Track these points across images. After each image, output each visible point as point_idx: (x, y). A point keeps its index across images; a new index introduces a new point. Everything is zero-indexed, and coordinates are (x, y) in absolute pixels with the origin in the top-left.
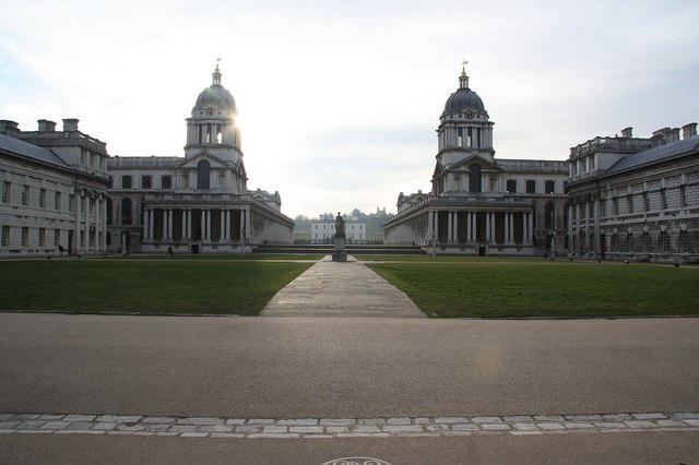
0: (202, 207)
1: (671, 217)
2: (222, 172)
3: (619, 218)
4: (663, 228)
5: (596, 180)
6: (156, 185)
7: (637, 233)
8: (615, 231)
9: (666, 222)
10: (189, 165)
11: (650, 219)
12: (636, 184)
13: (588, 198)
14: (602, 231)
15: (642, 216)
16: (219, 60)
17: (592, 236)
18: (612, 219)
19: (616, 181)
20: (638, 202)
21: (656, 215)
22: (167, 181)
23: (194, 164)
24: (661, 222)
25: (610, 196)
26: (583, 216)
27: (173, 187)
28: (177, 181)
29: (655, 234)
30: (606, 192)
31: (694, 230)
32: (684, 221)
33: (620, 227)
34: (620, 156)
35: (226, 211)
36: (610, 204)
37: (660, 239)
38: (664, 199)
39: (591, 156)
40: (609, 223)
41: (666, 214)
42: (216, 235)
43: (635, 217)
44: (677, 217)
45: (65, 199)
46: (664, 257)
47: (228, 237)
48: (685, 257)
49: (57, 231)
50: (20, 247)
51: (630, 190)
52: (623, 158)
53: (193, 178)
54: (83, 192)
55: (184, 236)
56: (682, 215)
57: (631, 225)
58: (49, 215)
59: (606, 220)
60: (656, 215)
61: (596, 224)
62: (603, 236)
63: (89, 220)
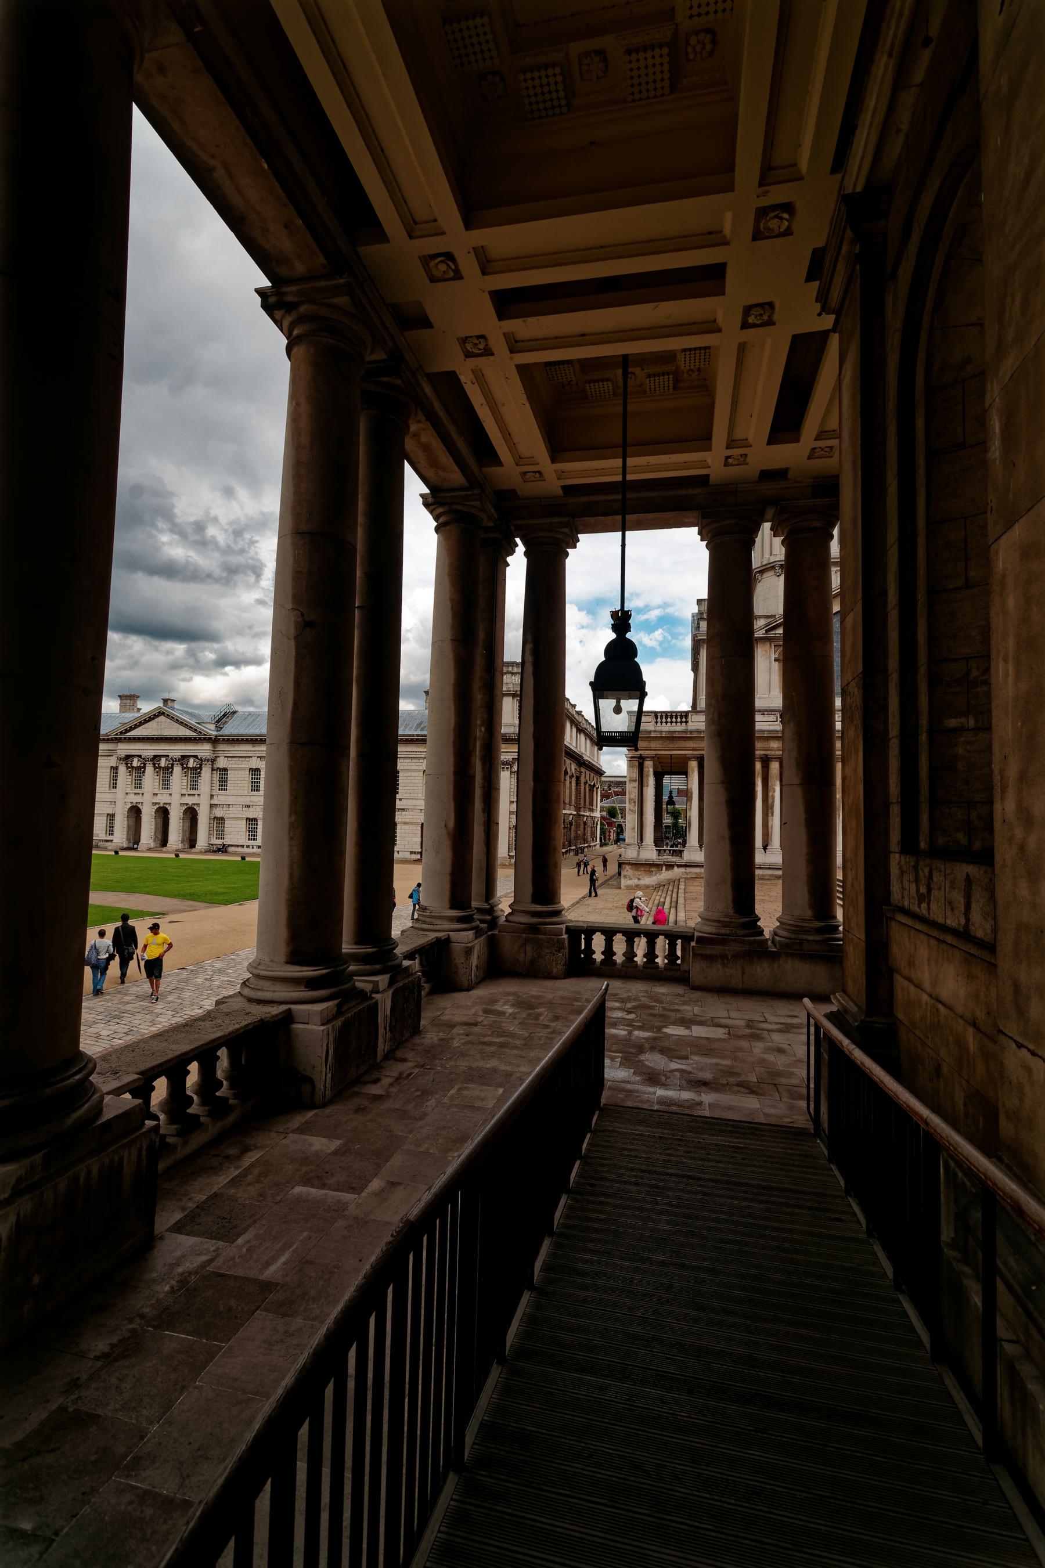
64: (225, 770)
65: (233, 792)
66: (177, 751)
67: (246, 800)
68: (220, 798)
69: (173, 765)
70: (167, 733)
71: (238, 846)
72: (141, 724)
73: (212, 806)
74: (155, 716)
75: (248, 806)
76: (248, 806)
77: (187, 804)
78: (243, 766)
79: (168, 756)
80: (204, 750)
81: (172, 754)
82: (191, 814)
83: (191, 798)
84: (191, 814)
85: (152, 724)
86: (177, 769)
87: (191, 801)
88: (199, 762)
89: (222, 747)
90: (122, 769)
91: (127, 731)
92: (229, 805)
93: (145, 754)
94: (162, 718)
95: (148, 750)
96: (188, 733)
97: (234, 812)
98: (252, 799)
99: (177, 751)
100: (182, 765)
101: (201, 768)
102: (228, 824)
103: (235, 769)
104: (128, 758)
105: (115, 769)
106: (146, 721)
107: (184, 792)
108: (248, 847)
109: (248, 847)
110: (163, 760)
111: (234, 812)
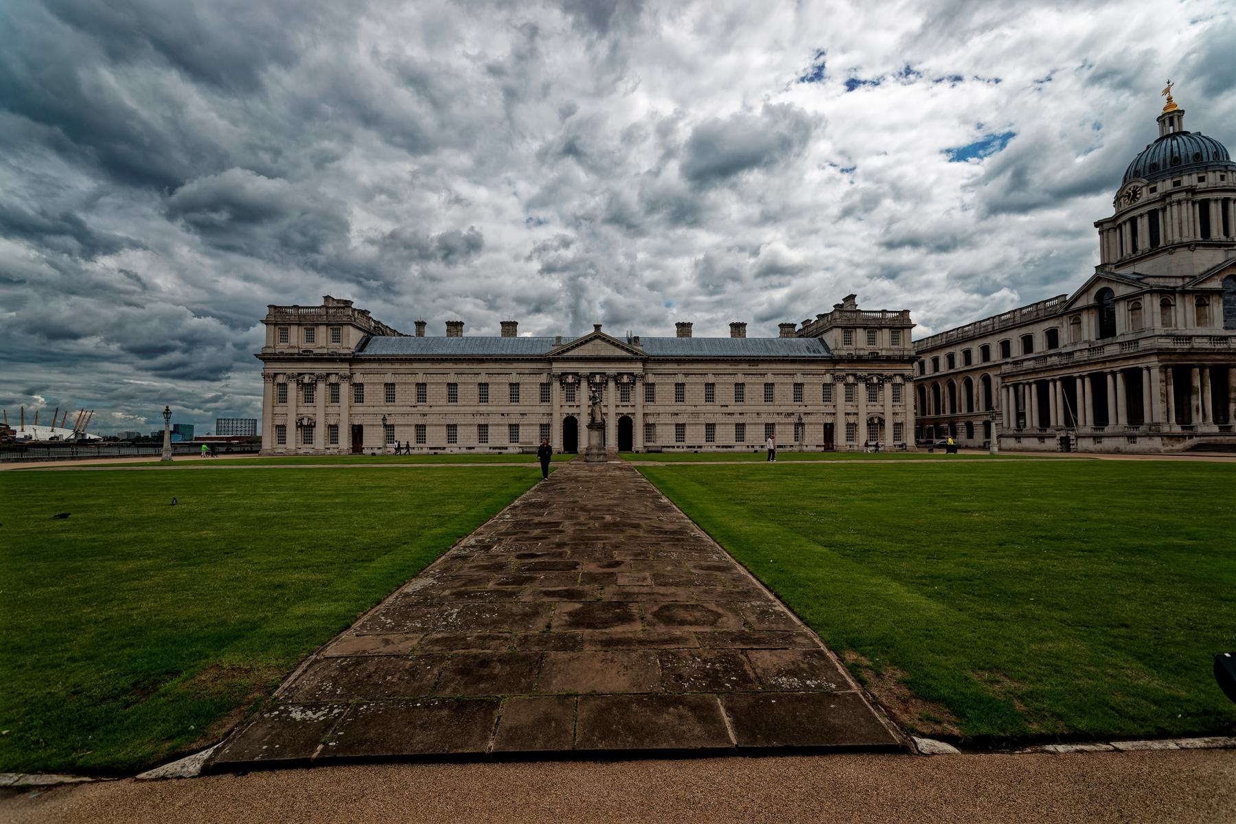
0: (1074, 372)
2: (1134, 303)
6: (1040, 345)
10: (1080, 304)
16: (1167, 91)
22: (1052, 336)
23: (1089, 299)
27: (1061, 344)
28: (1065, 334)
35: (1114, 374)
42: (1101, 417)
45: (813, 392)
47: (1123, 420)
49: (799, 425)
50: (733, 442)
53: (1089, 324)
54: (851, 380)
55: (1053, 423)
58: (783, 409)
63: (864, 407)
64: (653, 384)
65: (660, 403)
66: (612, 369)
67: (675, 409)
68: (651, 408)
69: (607, 381)
70: (603, 353)
71: (669, 447)
72: (577, 346)
73: (644, 414)
74: (591, 339)
75: (677, 414)
76: (677, 414)
77: (621, 414)
78: (669, 381)
79: (604, 374)
80: (637, 368)
81: (608, 372)
82: (625, 425)
83: (624, 408)
84: (625, 425)
85: (589, 346)
86: (612, 385)
87: (625, 411)
88: (632, 378)
89: (649, 366)
90: (556, 385)
91: (563, 352)
92: (659, 414)
93: (581, 372)
94: (598, 341)
95: (585, 369)
96: (624, 354)
97: (663, 419)
98: (679, 408)
99: (612, 369)
100: (616, 381)
101: (634, 383)
102: (659, 429)
103: (662, 384)
104: (564, 374)
105: (545, 387)
106: (582, 344)
107: (618, 403)
108: (678, 447)
109: (678, 447)
110: (598, 377)
111: (663, 419)
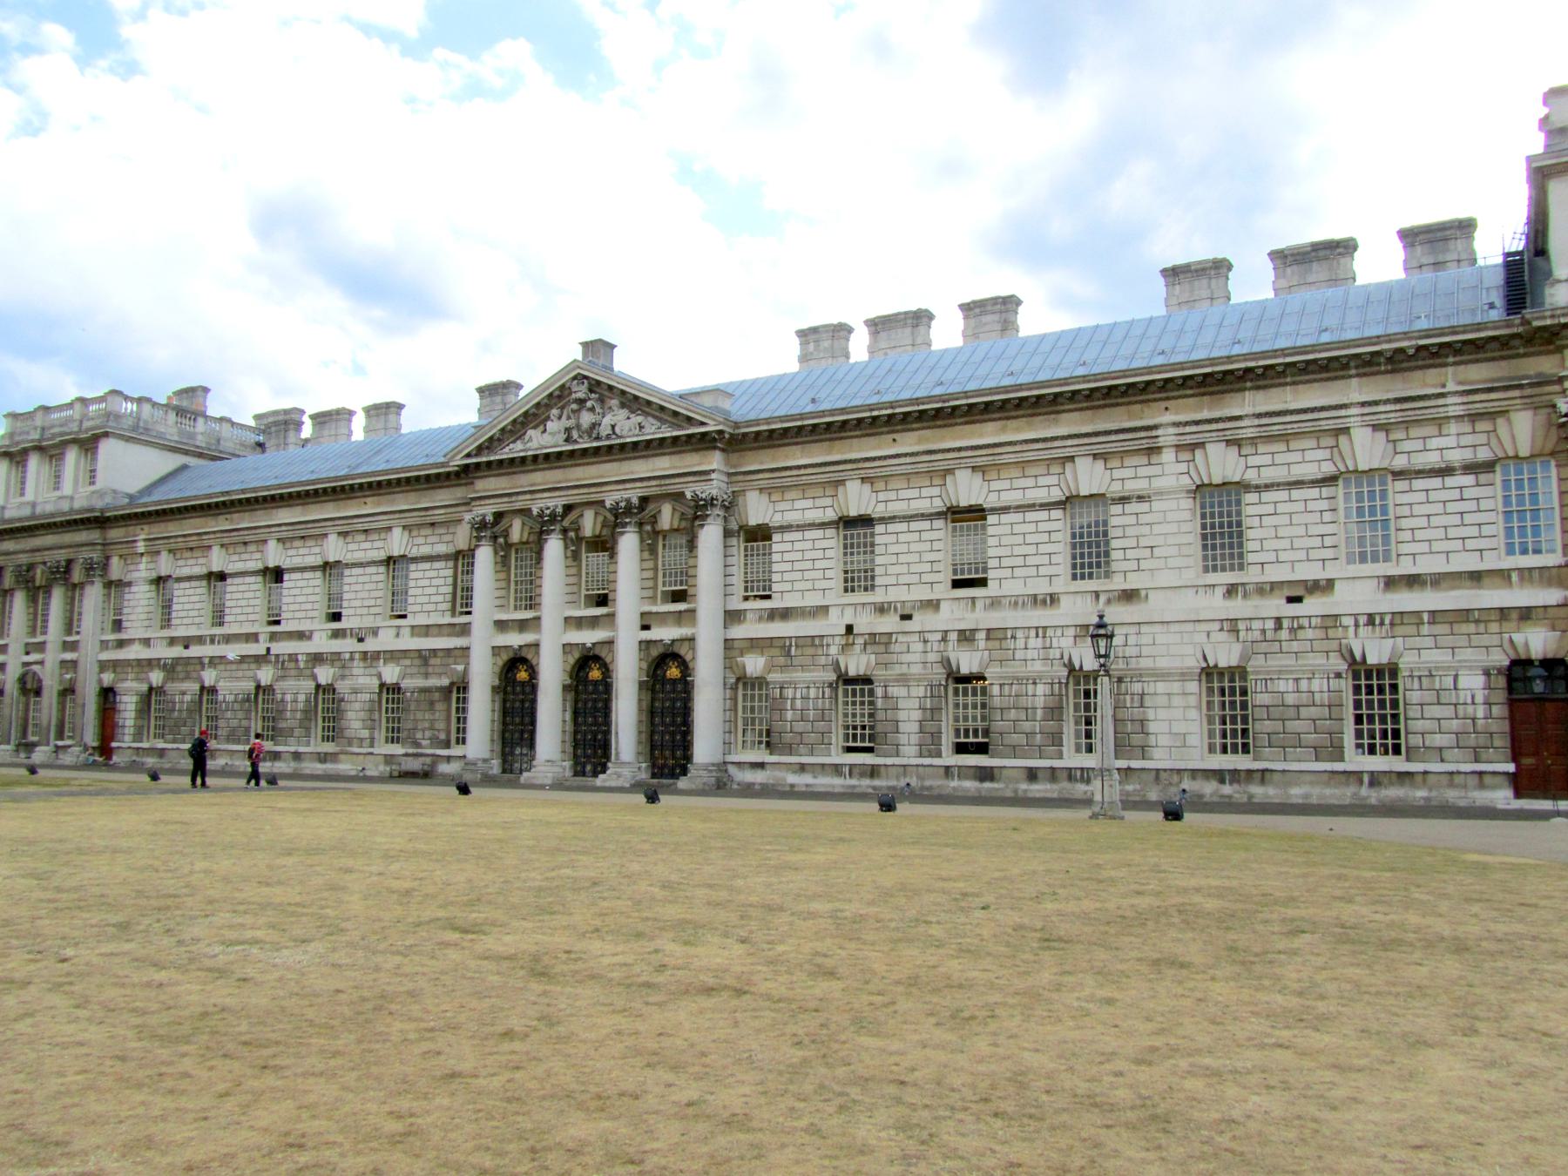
1: (347, 645)
3: (172, 641)
4: (325, 675)
5: (100, 521)
7: (231, 687)
8: (156, 677)
9: (335, 658)
11: (282, 648)
12: (238, 542)
13: (62, 573)
14: (108, 678)
15: (253, 637)
17: (68, 691)
18: (146, 642)
19: (173, 528)
20: (246, 600)
21: (301, 636)
24: (317, 659)
25: (143, 571)
26: (37, 623)
29: (296, 691)
30: (130, 557)
31: (420, 682)
32: (393, 656)
33: (172, 668)
34: (176, 461)
36: (140, 599)
37: (309, 713)
38: (334, 597)
39: (89, 444)
40: (134, 652)
41: (337, 634)
43: (228, 639)
44: (371, 645)
46: (323, 758)
48: (389, 759)
51: (218, 560)
52: (184, 467)
56: (386, 641)
57: (215, 661)
59: (121, 644)
60: (301, 636)
61: (90, 654)
62: (108, 695)
